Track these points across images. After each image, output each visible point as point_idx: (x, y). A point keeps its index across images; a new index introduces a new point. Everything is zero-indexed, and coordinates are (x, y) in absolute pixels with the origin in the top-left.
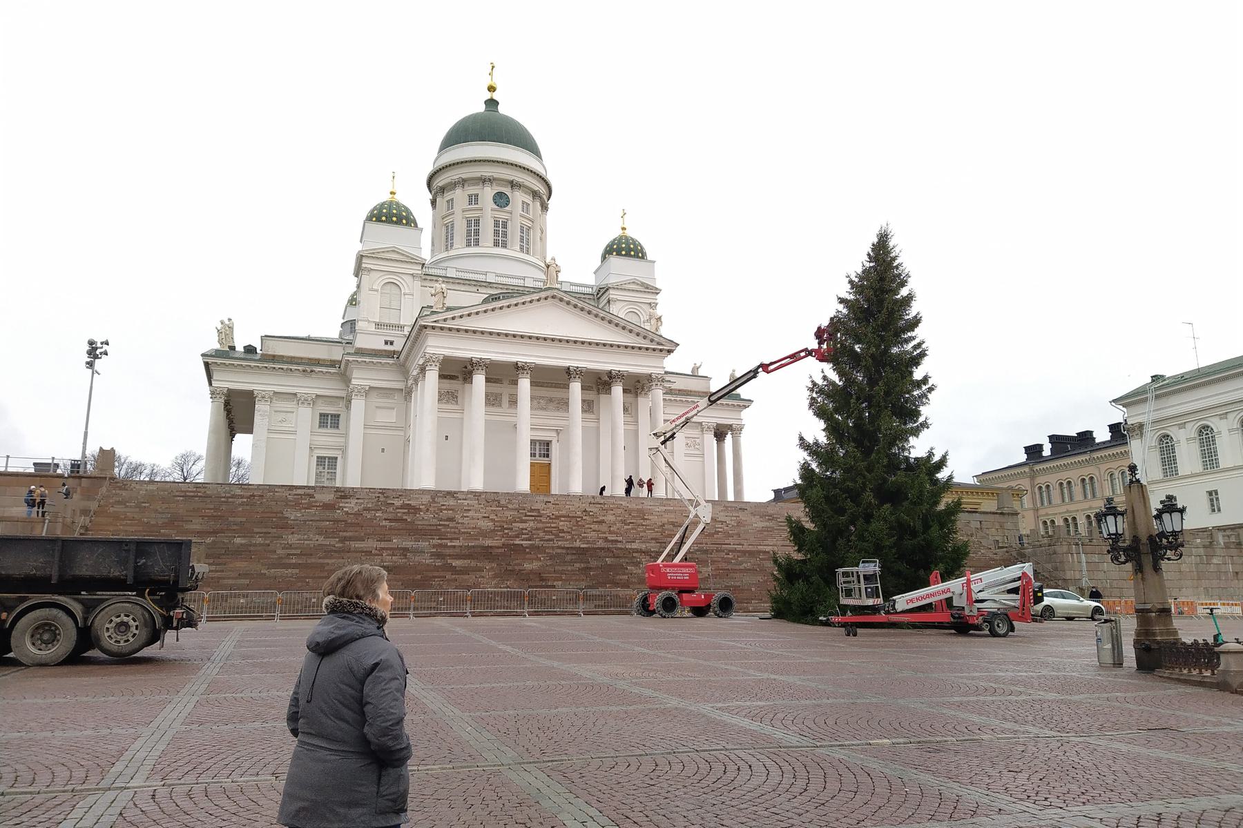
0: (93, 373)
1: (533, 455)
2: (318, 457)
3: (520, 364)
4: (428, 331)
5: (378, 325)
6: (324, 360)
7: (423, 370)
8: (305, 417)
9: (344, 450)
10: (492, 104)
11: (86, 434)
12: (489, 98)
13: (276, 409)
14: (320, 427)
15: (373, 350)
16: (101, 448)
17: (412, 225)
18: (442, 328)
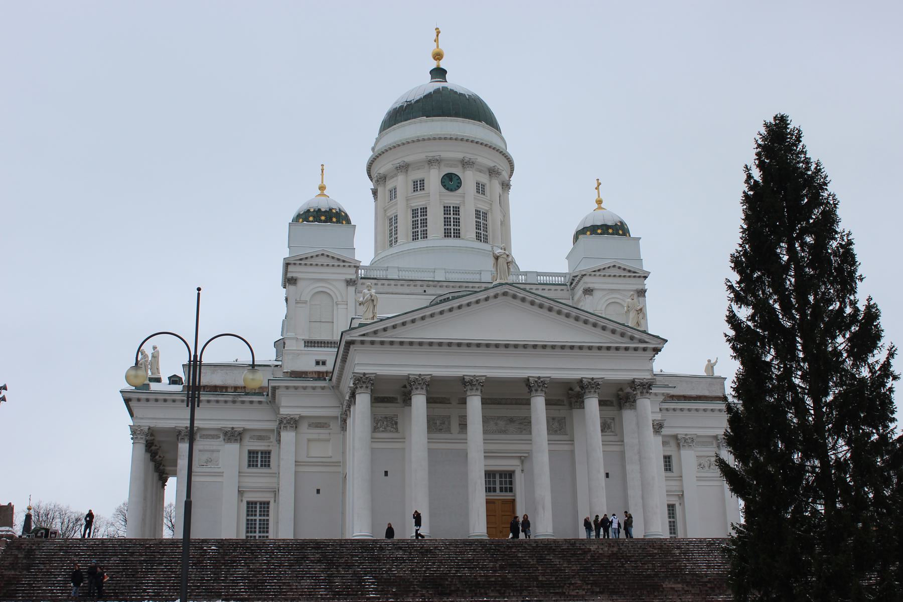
1: (488, 490)
2: (248, 503)
9: (276, 492)
10: (439, 73)
12: (434, 66)
13: (201, 447)
14: (249, 466)
17: (344, 222)
18: (372, 343)
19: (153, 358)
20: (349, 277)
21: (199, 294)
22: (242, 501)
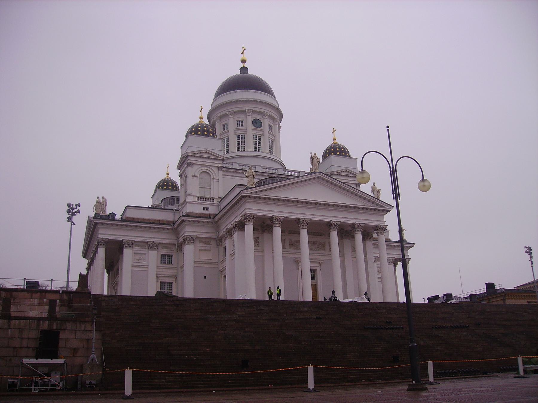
0: (72, 225)
3: (301, 220)
4: (247, 199)
5: (199, 198)
6: (163, 221)
7: (241, 226)
8: (153, 256)
9: (176, 278)
10: (244, 70)
11: (69, 264)
15: (197, 213)
16: (80, 273)
18: (255, 197)
19: (97, 203)
20: (220, 165)
21: (388, 130)
22: (158, 281)
